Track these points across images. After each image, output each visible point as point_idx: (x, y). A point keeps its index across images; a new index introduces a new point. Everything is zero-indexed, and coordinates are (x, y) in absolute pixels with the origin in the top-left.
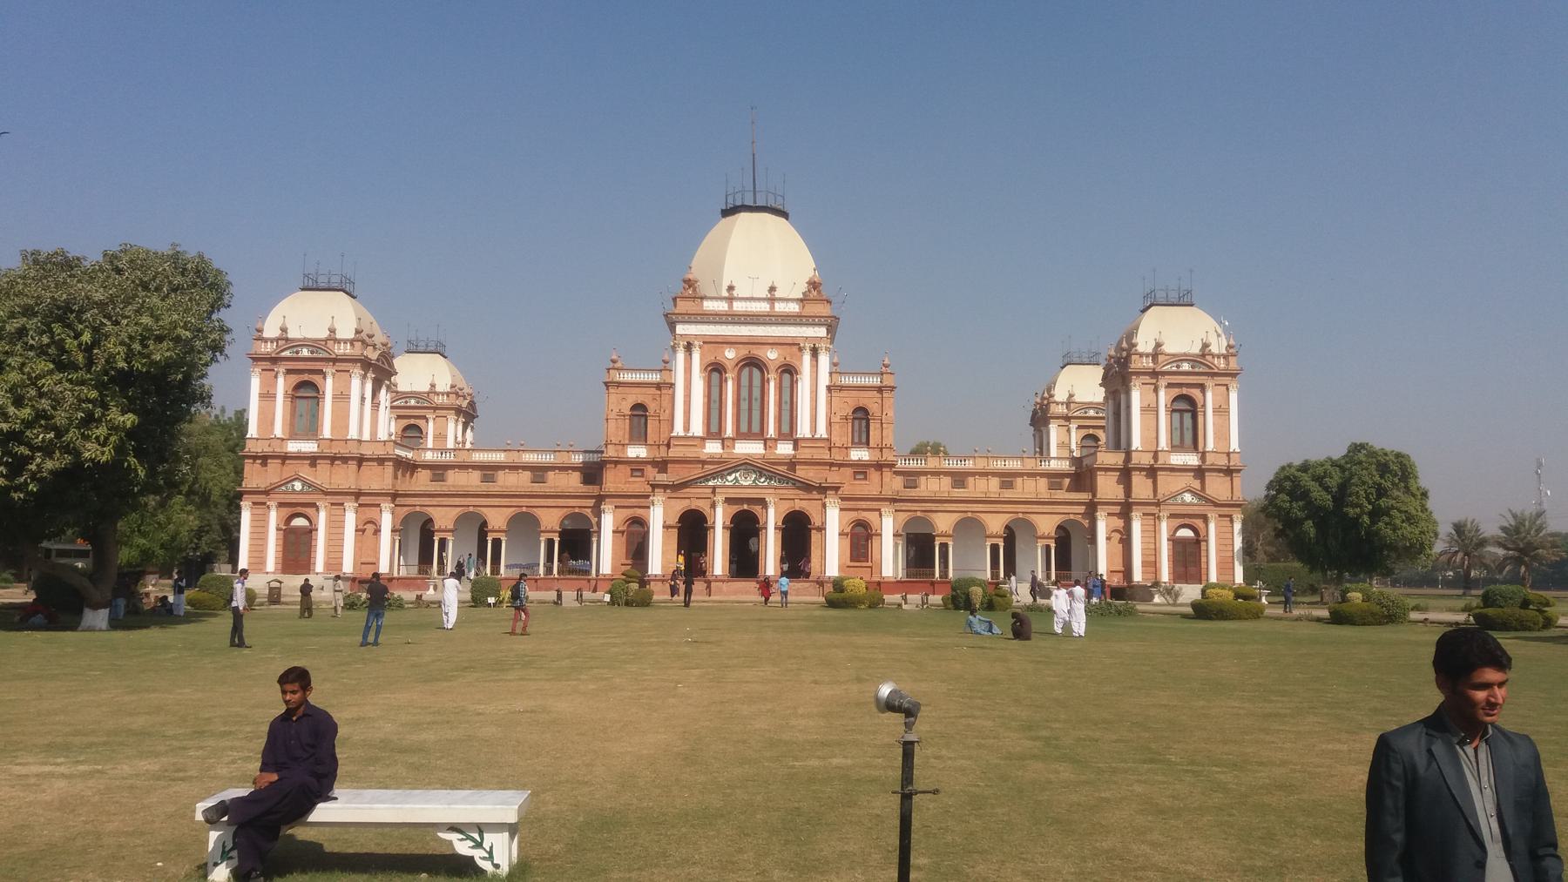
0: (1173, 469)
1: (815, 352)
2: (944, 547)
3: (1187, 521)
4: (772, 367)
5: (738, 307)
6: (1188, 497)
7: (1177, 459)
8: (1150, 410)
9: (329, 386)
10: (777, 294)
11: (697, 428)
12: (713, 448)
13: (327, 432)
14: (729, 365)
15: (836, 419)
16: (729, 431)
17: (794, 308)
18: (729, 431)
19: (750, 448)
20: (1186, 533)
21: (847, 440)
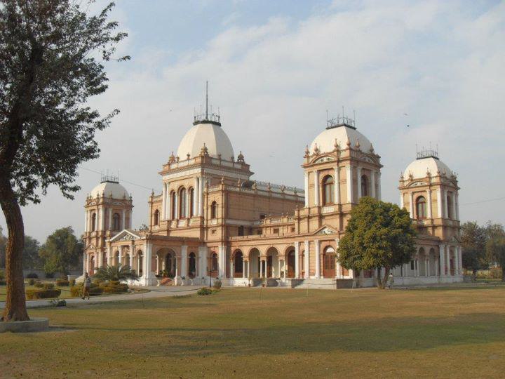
0: (321, 217)
1: (198, 179)
2: (246, 262)
3: (327, 243)
4: (187, 187)
5: (181, 165)
6: (326, 230)
7: (326, 210)
8: (311, 186)
9: (96, 213)
10: (190, 157)
11: (168, 217)
12: (173, 225)
13: (96, 230)
14: (176, 190)
15: (205, 208)
16: (177, 216)
17: (192, 162)
18: (177, 216)
19: (183, 223)
20: (330, 250)
21: (209, 217)
